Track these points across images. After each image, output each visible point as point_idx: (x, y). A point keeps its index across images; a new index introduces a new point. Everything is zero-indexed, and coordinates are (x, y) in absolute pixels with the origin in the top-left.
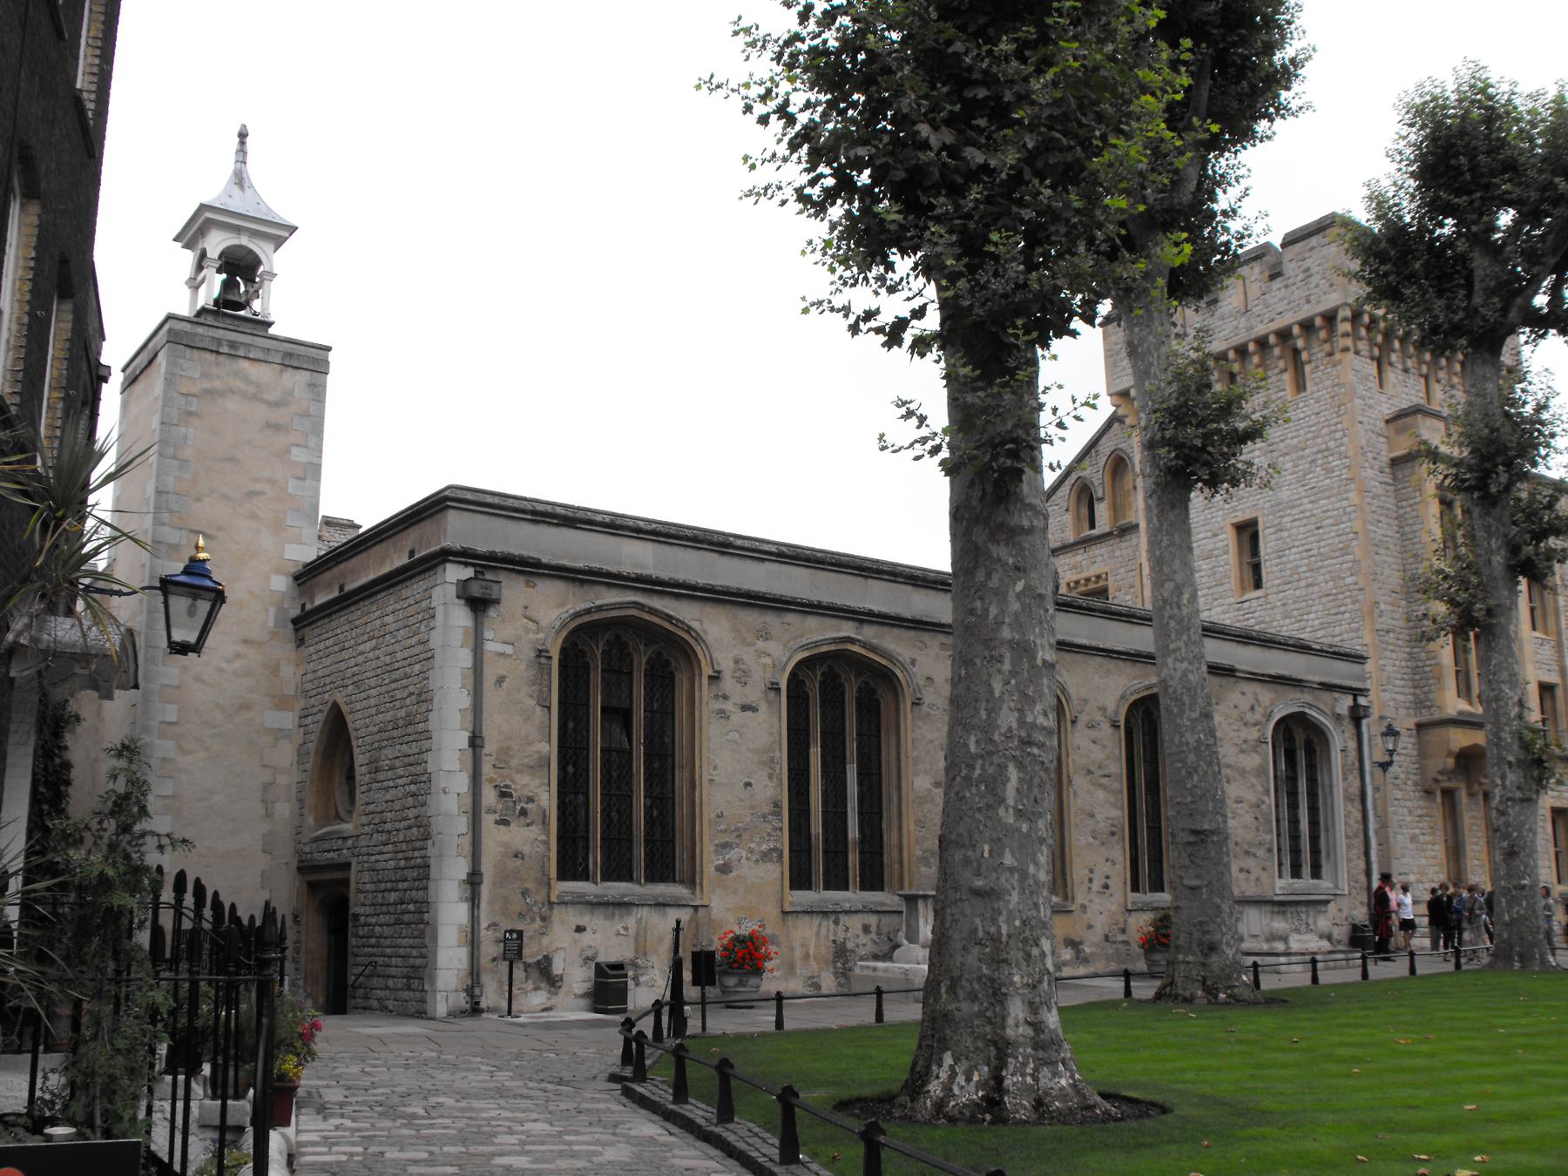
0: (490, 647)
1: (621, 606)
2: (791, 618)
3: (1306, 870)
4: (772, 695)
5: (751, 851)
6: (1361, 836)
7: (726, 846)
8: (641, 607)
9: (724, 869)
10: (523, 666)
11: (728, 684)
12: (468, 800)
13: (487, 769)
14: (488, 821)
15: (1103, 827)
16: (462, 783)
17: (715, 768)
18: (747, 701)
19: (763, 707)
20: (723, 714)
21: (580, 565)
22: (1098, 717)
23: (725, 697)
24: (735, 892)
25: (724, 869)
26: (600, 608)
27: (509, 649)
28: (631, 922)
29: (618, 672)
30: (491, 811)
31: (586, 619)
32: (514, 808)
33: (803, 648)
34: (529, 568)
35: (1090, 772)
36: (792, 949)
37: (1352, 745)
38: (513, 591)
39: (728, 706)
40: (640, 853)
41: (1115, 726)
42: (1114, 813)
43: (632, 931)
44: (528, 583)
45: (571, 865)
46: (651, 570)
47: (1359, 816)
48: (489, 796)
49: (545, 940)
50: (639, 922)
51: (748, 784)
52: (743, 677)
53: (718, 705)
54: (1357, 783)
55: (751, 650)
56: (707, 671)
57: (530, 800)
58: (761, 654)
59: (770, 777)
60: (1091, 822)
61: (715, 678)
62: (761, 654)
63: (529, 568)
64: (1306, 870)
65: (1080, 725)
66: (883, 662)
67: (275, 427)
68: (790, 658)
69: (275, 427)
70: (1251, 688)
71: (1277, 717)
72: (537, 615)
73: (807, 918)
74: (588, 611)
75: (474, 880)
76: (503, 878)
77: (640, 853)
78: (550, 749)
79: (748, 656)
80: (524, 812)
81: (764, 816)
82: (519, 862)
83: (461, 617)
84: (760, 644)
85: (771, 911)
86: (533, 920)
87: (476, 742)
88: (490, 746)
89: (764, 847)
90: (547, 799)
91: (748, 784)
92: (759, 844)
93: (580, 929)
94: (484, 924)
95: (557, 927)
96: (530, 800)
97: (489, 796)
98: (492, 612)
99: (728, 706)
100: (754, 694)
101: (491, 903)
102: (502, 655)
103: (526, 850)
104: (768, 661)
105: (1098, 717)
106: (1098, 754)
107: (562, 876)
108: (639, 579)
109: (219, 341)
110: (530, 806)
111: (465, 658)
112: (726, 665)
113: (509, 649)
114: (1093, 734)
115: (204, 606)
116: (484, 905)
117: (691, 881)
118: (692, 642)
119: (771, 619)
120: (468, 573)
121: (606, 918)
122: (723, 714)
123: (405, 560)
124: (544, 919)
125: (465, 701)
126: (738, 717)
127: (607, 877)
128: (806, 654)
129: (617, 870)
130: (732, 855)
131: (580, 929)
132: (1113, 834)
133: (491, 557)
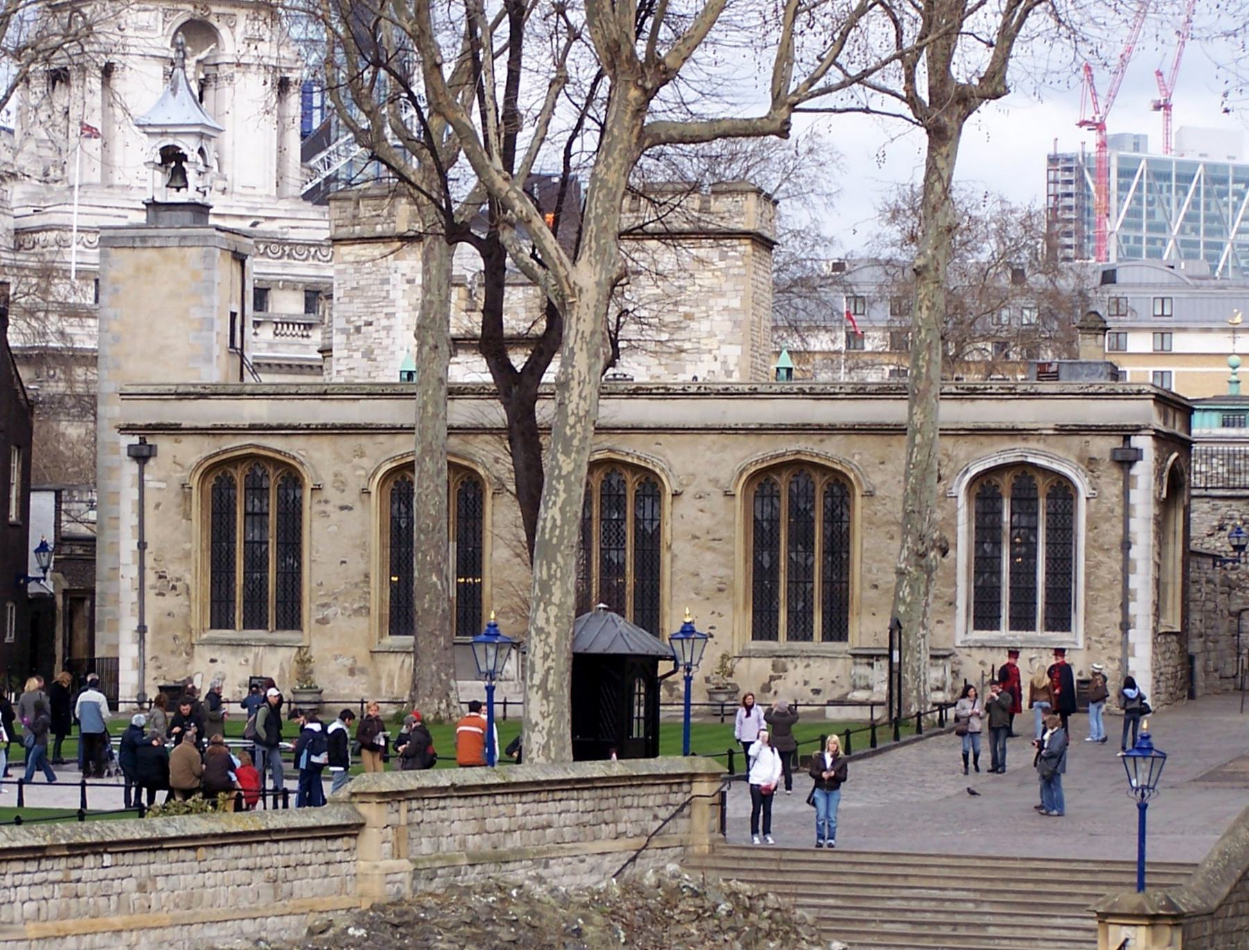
0: (150, 484)
1: (241, 448)
2: (381, 438)
4: (365, 496)
5: (345, 609)
6: (1119, 588)
7: (324, 606)
8: (258, 447)
9: (323, 621)
10: (173, 495)
11: (329, 492)
13: (149, 561)
14: (150, 595)
15: (708, 584)
16: (134, 572)
17: (317, 552)
18: (346, 503)
19: (358, 506)
20: (324, 514)
21: (209, 425)
22: (709, 488)
23: (326, 502)
24: (331, 637)
25: (323, 621)
26: (225, 451)
27: (163, 485)
28: (250, 654)
29: (256, 489)
30: (153, 587)
31: (217, 459)
32: (168, 585)
33: (392, 459)
34: (173, 430)
35: (695, 537)
36: (379, 678)
37: (1112, 491)
38: (164, 445)
39: (329, 508)
40: (271, 612)
41: (728, 495)
42: (722, 572)
43: (251, 662)
44: (176, 441)
45: (221, 618)
46: (265, 421)
47: (1117, 567)
48: (151, 579)
49: (189, 667)
50: (256, 655)
51: (343, 562)
52: (341, 486)
53: (322, 507)
54: (1120, 531)
55: (348, 466)
56: (309, 484)
57: (178, 580)
58: (356, 468)
59: (362, 556)
60: (695, 580)
61: (317, 489)
62: (356, 468)
63: (173, 430)
65: (685, 497)
66: (466, 463)
68: (379, 468)
71: (974, 471)
72: (181, 459)
73: (393, 656)
74: (217, 454)
75: (142, 629)
76: (160, 629)
77: (271, 612)
79: (346, 471)
80: (174, 588)
81: (356, 585)
82: (170, 619)
83: (132, 468)
84: (356, 461)
85: (362, 652)
86: (181, 654)
87: (142, 545)
89: (356, 606)
91: (343, 562)
92: (352, 604)
93: (213, 661)
94: (148, 656)
95: (197, 659)
96: (178, 580)
98: (151, 462)
99: (329, 508)
100: (350, 497)
101: (153, 644)
102: (159, 489)
103: (175, 611)
104: (362, 472)
105: (709, 488)
106: (706, 521)
108: (253, 427)
110: (178, 584)
112: (327, 479)
113: (163, 485)
114: (701, 504)
116: (148, 646)
118: (298, 466)
119: (364, 441)
120: (135, 440)
121: (233, 653)
122: (324, 514)
124: (187, 654)
125: (135, 521)
126: (336, 515)
127: (246, 626)
128: (394, 465)
129: (255, 619)
130: (329, 612)
131: (213, 661)
132: (720, 590)
133: (140, 428)
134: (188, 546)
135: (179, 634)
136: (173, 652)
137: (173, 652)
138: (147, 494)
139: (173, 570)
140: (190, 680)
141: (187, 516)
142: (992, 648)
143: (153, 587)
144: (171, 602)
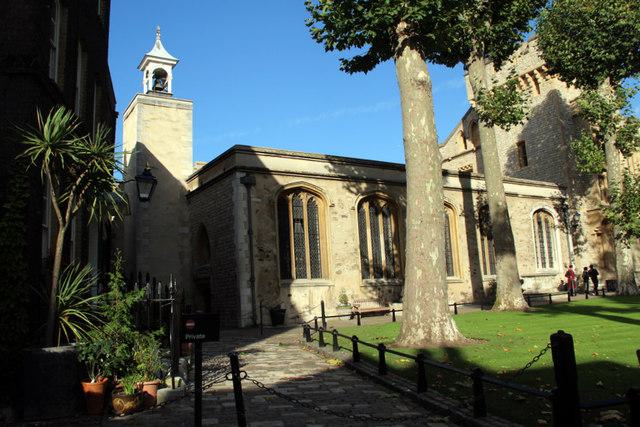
0: (253, 200)
3: (548, 264)
9: (339, 273)
12: (248, 252)
13: (254, 242)
14: (256, 260)
20: (336, 219)
25: (339, 273)
28: (307, 291)
30: (257, 256)
32: (264, 255)
39: (337, 216)
48: (256, 251)
64: (548, 264)
67: (176, 130)
69: (176, 130)
70: (524, 200)
75: (252, 280)
78: (276, 234)
80: (268, 256)
83: (242, 190)
87: (250, 232)
88: (255, 234)
90: (276, 251)
94: (256, 295)
97: (256, 251)
99: (337, 216)
100: (346, 211)
101: (258, 288)
107: (282, 279)
109: (154, 101)
111: (244, 204)
115: (150, 186)
117: (327, 277)
120: (244, 174)
123: (221, 172)
133: (251, 168)
134: (274, 234)
135: (272, 281)
136: (269, 292)
137: (269, 292)
138: (254, 209)
139: (267, 246)
140: (279, 306)
141: (273, 217)
142: (538, 276)
143: (257, 256)
144: (267, 264)
